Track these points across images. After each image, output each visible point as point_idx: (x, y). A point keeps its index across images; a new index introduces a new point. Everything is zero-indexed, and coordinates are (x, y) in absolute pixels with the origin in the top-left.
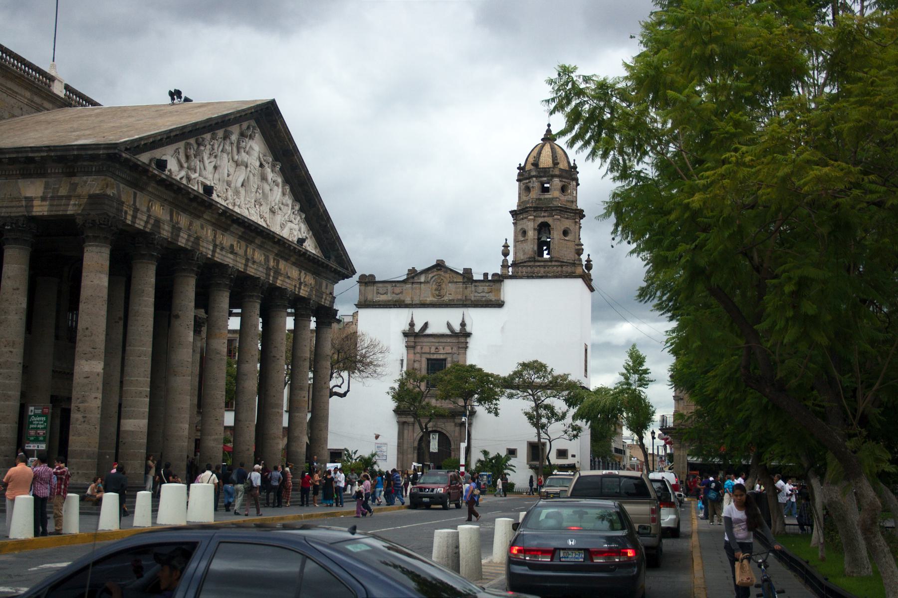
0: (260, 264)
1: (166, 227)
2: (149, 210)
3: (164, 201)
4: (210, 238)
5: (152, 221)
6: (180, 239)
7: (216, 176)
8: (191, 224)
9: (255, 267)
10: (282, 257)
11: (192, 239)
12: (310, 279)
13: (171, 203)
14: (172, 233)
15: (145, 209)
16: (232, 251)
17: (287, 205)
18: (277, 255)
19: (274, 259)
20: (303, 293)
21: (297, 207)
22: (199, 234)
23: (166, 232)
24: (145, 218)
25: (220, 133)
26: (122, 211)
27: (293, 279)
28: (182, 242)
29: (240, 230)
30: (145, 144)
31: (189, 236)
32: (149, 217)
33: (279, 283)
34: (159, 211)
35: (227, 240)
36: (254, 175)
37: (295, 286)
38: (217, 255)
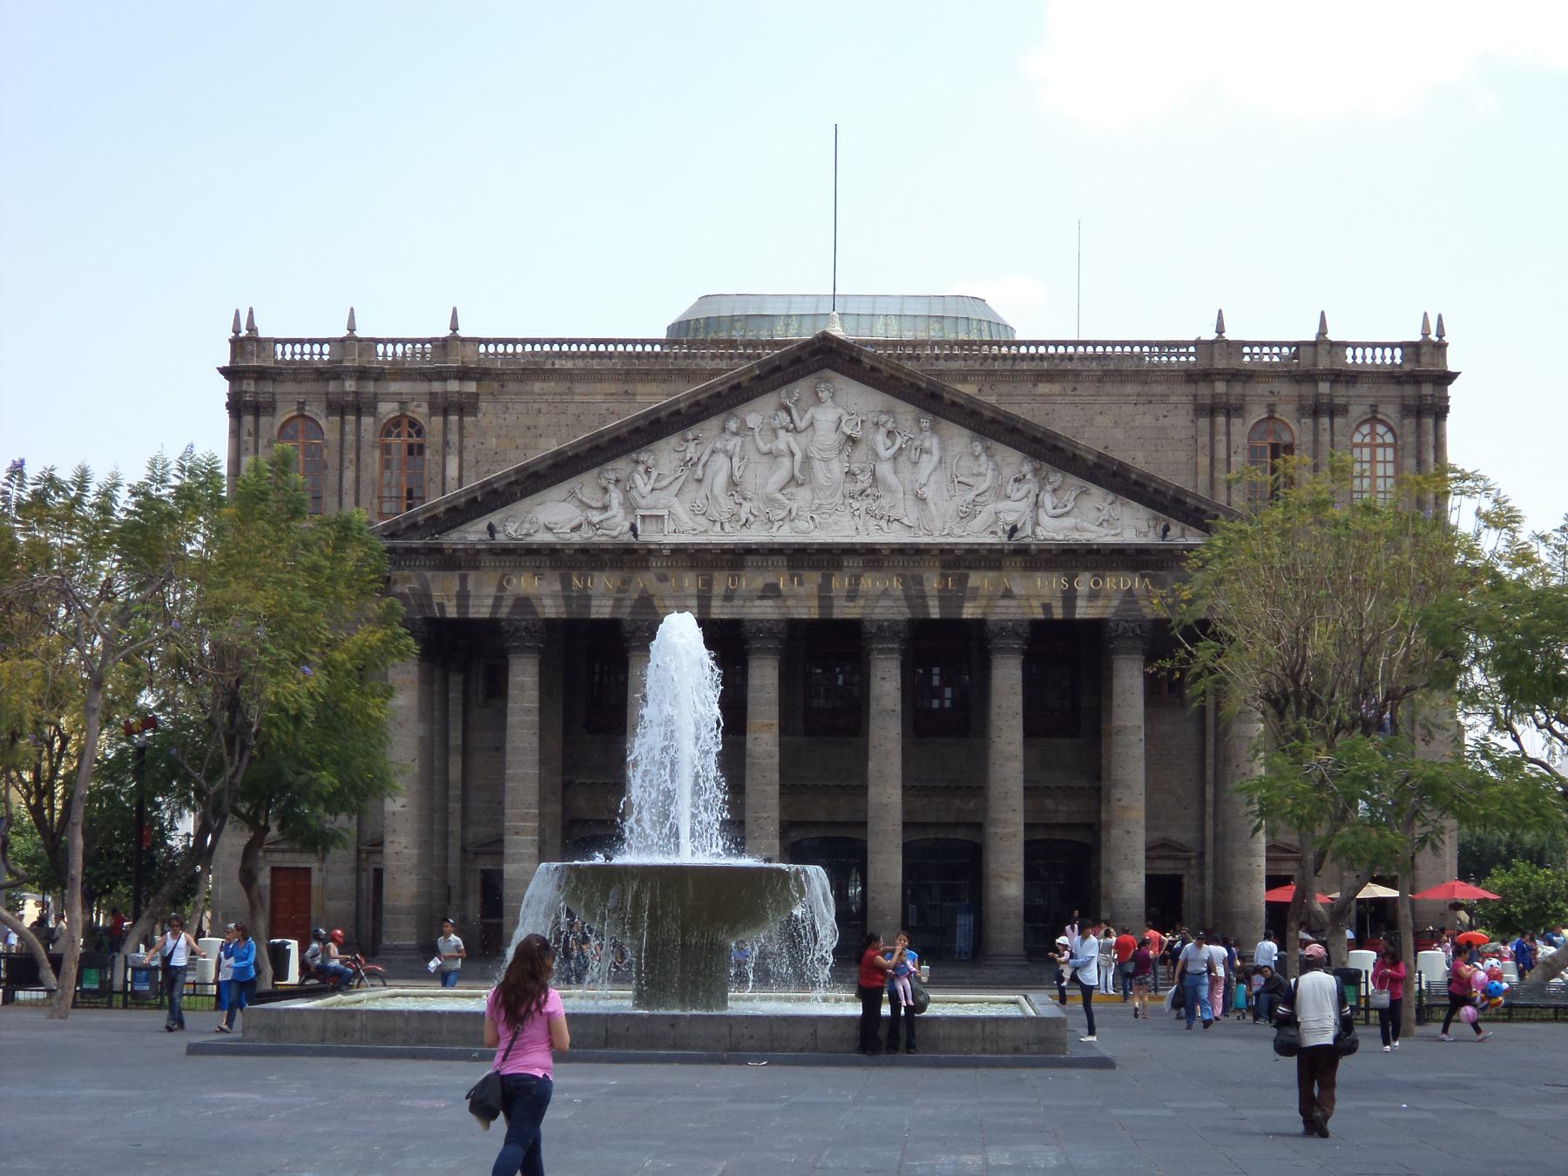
0: (885, 594)
1: (547, 602)
2: (501, 588)
3: (537, 571)
4: (693, 590)
5: (507, 604)
6: (593, 610)
7: (702, 493)
8: (624, 582)
9: (862, 603)
10: (970, 568)
11: (628, 603)
12: (1117, 583)
13: (552, 567)
14: (568, 606)
15: (491, 590)
16: (771, 592)
17: (980, 474)
18: (944, 566)
19: (944, 577)
20: (1083, 611)
21: (1027, 468)
22: (651, 592)
23: (551, 609)
24: (490, 602)
25: (712, 424)
26: (430, 606)
27: (1028, 598)
28: (601, 609)
29: (782, 561)
30: (427, 520)
31: (616, 600)
32: (498, 600)
33: (969, 611)
34: (525, 584)
35: (752, 580)
36: (826, 461)
37: (1047, 608)
38: (714, 610)
